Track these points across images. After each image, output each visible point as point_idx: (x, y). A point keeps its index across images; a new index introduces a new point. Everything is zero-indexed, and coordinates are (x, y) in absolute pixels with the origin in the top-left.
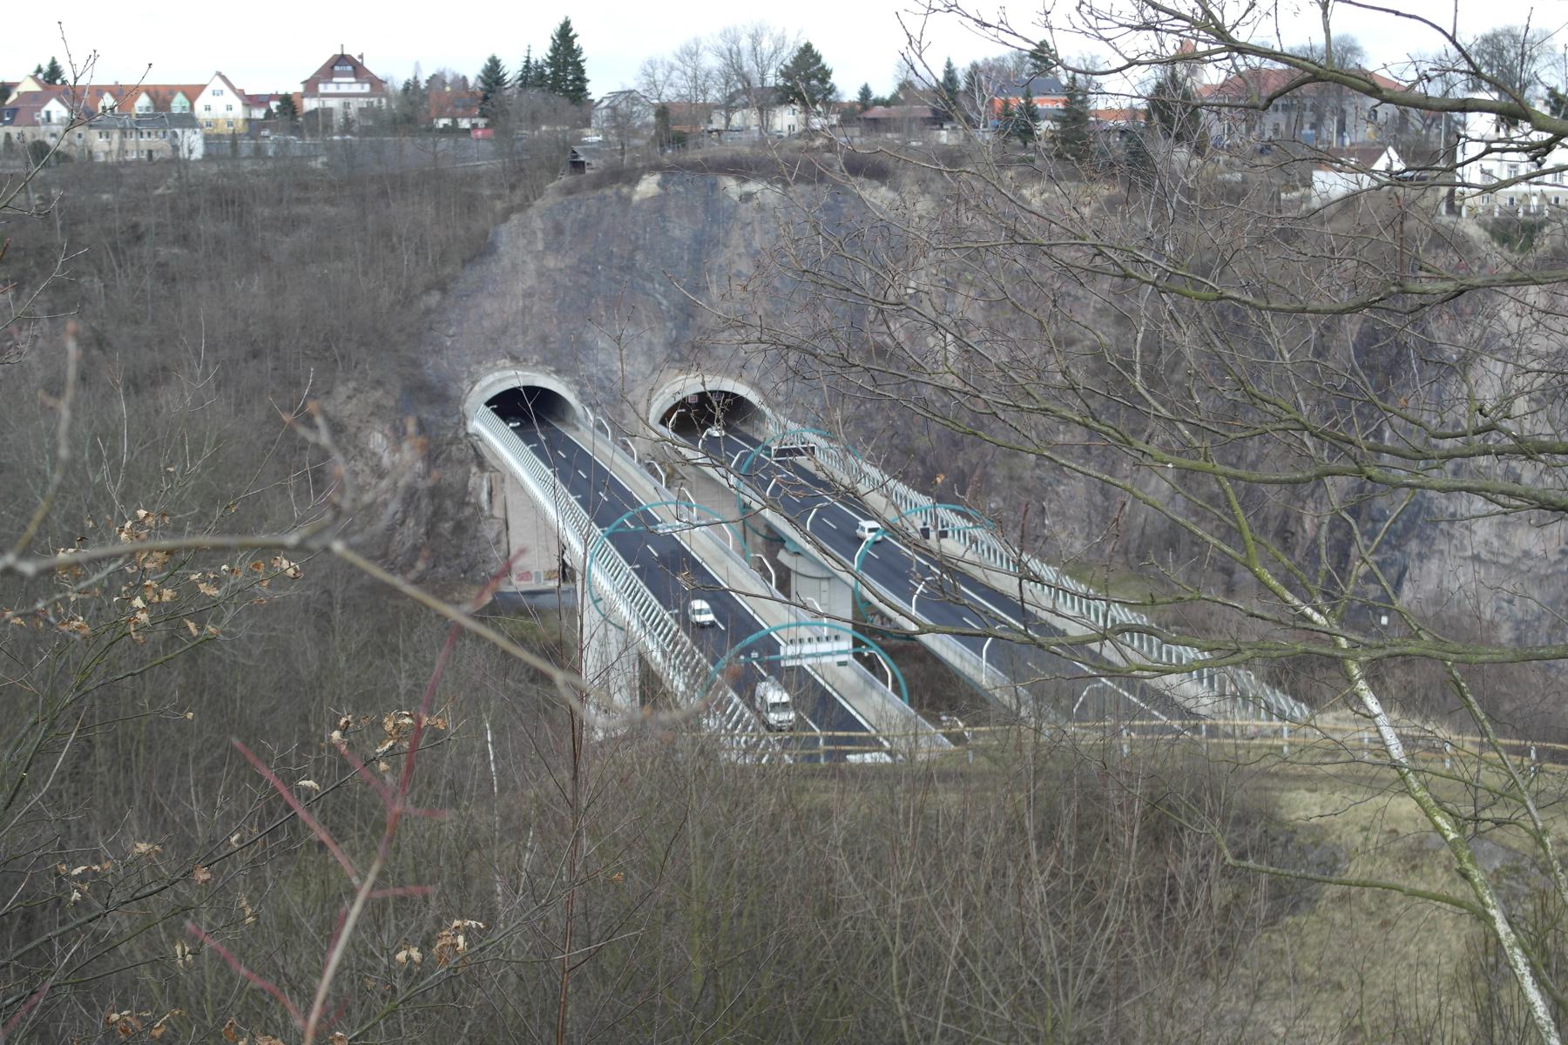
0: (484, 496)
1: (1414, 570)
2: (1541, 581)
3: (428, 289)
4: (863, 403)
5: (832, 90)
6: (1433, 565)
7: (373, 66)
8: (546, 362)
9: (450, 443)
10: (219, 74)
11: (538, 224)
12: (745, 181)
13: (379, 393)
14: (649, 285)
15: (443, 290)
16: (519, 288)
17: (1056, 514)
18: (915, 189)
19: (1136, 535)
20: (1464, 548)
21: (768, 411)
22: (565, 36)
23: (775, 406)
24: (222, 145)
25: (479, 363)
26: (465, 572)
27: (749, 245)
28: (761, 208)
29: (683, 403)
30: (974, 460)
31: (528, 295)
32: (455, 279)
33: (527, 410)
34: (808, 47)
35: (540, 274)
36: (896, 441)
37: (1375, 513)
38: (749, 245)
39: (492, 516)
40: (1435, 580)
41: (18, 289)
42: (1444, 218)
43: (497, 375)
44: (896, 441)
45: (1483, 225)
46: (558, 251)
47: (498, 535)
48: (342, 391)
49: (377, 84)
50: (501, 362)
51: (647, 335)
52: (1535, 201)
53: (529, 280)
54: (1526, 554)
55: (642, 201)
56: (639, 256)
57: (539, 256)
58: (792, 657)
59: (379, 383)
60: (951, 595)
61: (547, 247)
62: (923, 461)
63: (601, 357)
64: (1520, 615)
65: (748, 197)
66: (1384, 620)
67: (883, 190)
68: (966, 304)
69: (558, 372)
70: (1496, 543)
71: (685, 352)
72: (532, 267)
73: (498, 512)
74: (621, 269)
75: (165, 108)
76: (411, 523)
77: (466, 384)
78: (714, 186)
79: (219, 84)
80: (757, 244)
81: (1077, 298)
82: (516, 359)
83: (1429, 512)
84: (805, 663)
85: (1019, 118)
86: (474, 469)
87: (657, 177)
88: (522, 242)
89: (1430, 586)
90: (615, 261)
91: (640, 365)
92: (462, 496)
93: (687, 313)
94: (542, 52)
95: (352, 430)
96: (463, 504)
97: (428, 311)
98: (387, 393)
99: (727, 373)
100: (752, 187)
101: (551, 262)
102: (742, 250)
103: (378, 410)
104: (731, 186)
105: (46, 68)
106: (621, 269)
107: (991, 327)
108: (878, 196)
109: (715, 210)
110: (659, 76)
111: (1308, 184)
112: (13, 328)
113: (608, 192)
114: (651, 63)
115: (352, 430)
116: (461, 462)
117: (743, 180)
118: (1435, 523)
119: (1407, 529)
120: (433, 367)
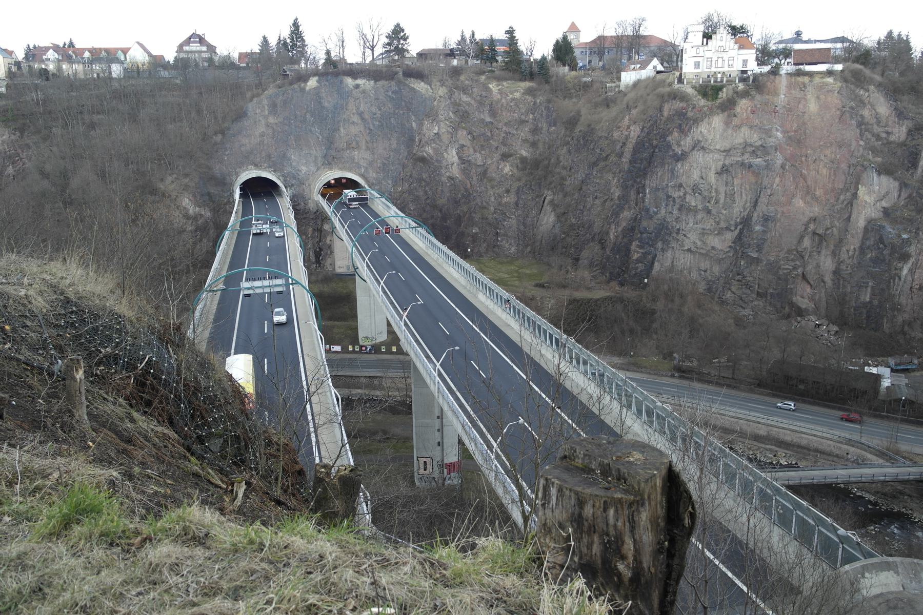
1: (659, 257)
2: (720, 261)
3: (216, 134)
4: (412, 183)
6: (669, 254)
7: (209, 39)
8: (269, 167)
9: (225, 204)
10: (138, 43)
11: (265, 102)
13: (187, 180)
15: (223, 133)
16: (257, 133)
17: (504, 235)
18: (438, 84)
19: (538, 244)
20: (683, 246)
21: (366, 186)
22: (296, 25)
24: (133, 72)
27: (358, 109)
28: (364, 92)
30: (466, 210)
31: (262, 135)
32: (228, 129)
34: (398, 25)
35: (268, 125)
36: (428, 201)
38: (358, 109)
40: (670, 261)
41: (22, 133)
42: (676, 86)
44: (428, 201)
45: (694, 87)
46: (275, 114)
48: (169, 179)
49: (212, 49)
52: (719, 76)
53: (261, 129)
54: (713, 248)
56: (308, 116)
57: (266, 117)
59: (187, 175)
62: (441, 211)
64: (710, 278)
65: (357, 86)
66: (646, 281)
67: (422, 84)
68: (463, 137)
69: (275, 171)
70: (699, 243)
72: (263, 122)
75: (110, 56)
76: (205, 240)
77: (234, 177)
78: (341, 82)
80: (361, 109)
81: (514, 135)
82: (257, 166)
83: (667, 228)
85: (498, 58)
87: (316, 78)
88: (258, 111)
89: (668, 264)
93: (330, 142)
94: (286, 33)
95: (174, 197)
97: (216, 144)
98: (192, 180)
99: (350, 170)
100: (360, 81)
101: (271, 120)
103: (186, 188)
104: (349, 81)
105: (67, 43)
108: (420, 86)
109: (343, 94)
111: (619, 79)
112: (20, 151)
113: (296, 86)
115: (174, 197)
117: (355, 78)
118: (670, 234)
119: (657, 237)
120: (218, 169)
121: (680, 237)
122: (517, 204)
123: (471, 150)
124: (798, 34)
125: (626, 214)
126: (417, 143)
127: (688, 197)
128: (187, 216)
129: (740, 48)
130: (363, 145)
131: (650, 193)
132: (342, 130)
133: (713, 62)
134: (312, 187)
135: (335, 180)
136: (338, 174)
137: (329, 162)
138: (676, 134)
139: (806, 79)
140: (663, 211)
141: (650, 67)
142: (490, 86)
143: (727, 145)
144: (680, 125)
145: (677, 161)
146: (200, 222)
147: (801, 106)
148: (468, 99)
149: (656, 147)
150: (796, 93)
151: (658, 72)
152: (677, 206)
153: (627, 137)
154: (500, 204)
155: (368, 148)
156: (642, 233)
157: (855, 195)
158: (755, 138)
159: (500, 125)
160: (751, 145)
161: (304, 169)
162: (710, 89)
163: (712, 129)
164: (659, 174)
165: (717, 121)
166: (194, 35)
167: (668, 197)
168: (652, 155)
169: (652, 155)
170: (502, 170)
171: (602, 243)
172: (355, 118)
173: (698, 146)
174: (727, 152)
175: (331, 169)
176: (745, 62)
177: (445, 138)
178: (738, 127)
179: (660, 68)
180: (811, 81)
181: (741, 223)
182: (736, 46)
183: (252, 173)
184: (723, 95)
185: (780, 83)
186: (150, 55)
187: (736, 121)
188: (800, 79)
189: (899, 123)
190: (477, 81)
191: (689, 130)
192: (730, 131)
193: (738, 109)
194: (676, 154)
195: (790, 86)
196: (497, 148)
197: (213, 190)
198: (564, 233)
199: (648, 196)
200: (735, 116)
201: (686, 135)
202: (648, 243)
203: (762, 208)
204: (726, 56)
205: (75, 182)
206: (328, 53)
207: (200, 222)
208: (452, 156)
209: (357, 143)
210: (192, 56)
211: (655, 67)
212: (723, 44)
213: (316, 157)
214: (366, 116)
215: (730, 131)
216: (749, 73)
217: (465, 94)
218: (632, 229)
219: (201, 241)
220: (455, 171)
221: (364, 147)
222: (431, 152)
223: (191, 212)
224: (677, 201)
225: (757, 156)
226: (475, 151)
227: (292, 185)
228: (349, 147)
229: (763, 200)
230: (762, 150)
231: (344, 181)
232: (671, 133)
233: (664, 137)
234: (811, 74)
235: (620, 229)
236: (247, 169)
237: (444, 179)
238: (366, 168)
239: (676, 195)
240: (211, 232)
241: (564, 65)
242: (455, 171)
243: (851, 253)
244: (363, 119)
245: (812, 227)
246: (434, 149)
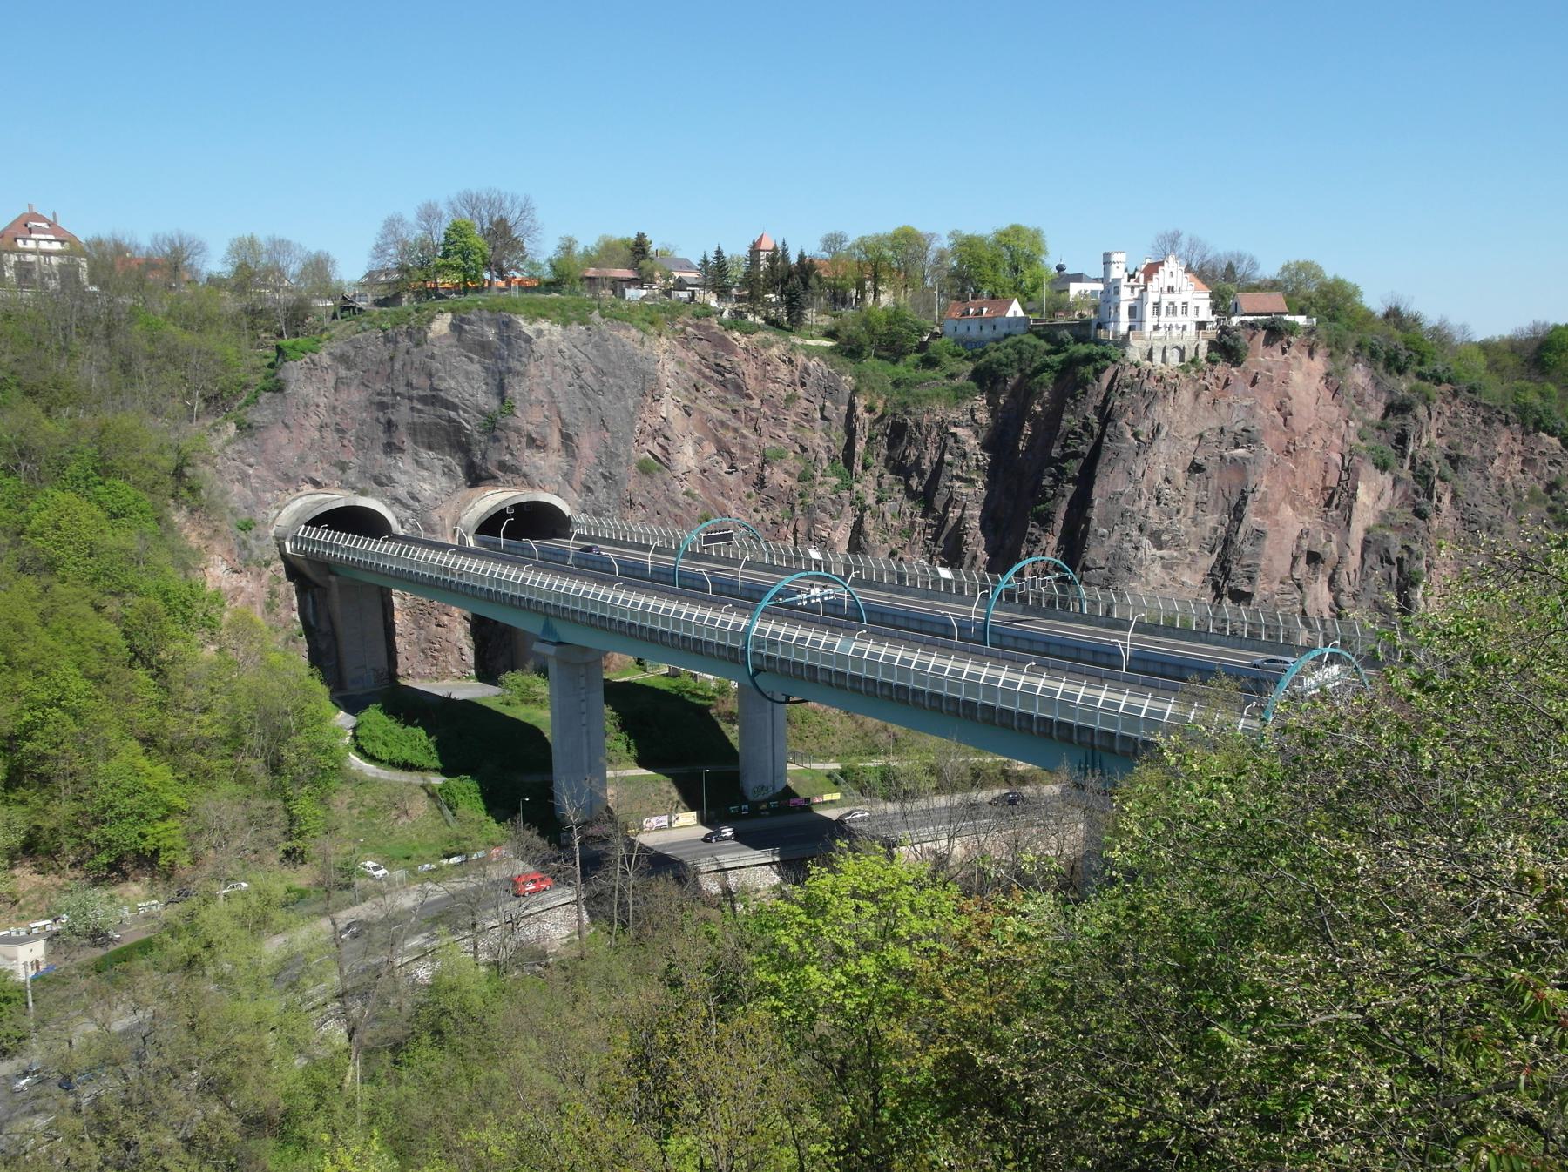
12: (534, 320)
65: (540, 333)
100: (544, 325)
124: (1060, 268)
130: (555, 440)
157: (1353, 496)
183: (337, 498)
203: (1251, 519)
209: (544, 439)
210: (31, 258)
212: (1171, 282)
229: (1250, 508)
230: (1245, 437)
243: (1352, 576)
245: (1305, 543)
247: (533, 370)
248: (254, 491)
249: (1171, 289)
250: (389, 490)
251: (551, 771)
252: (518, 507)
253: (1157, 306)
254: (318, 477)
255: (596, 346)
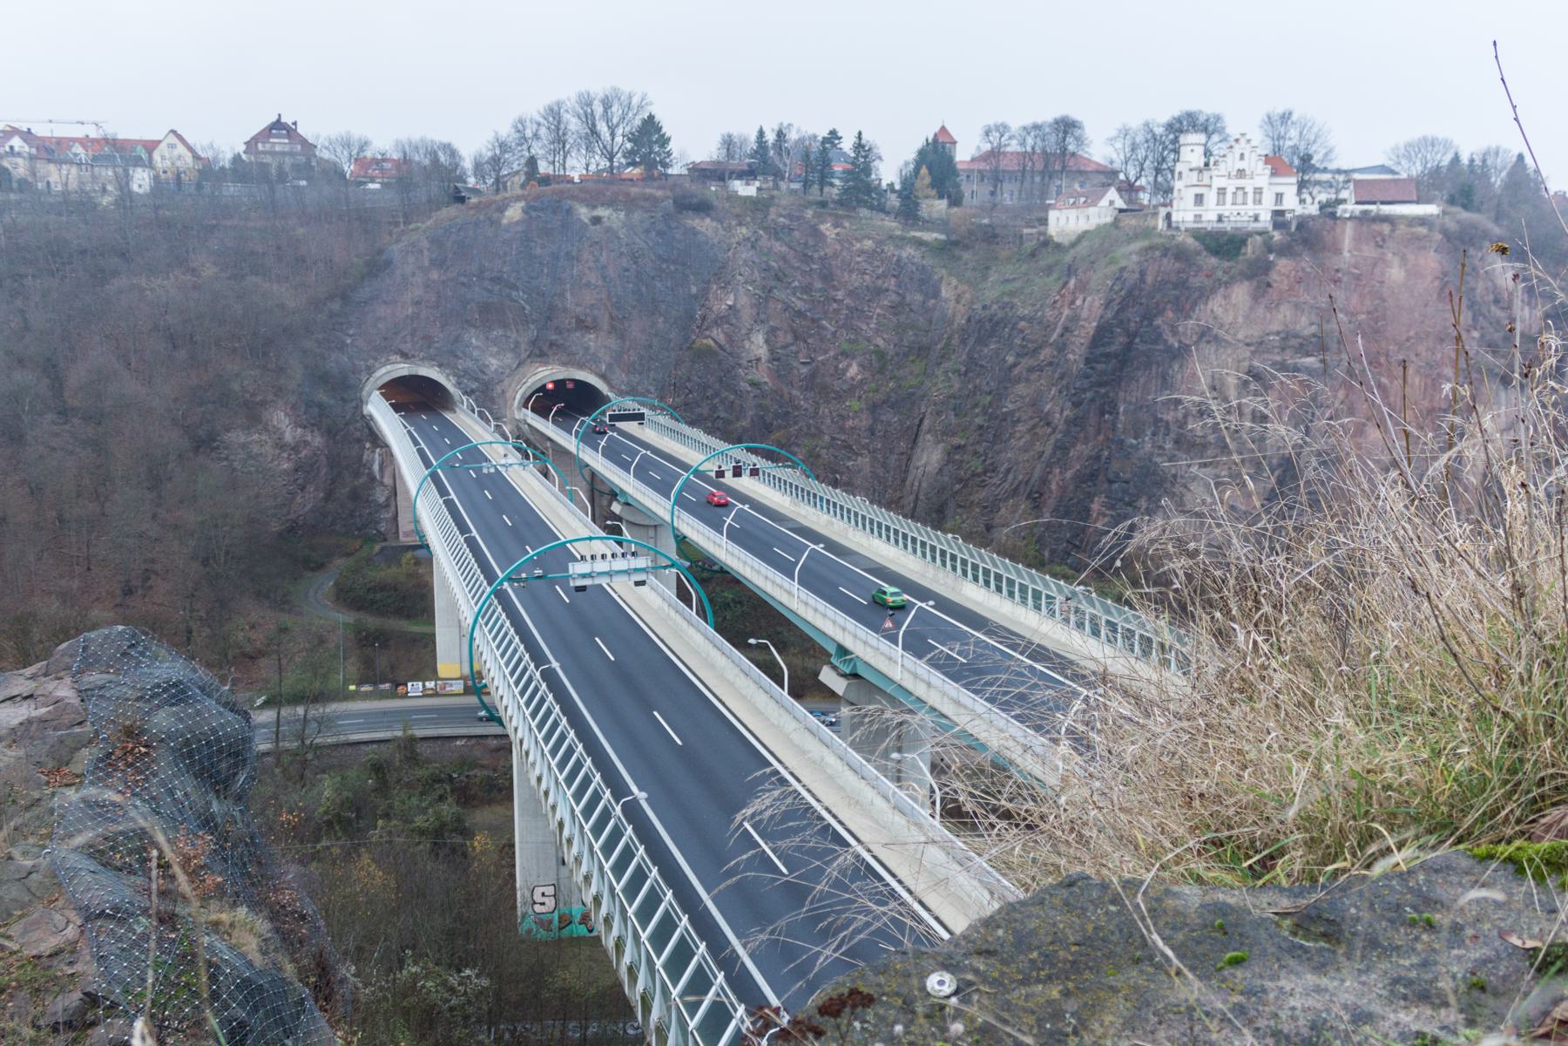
0: (376, 467)
5: (669, 154)
10: (173, 132)
12: (594, 207)
14: (514, 294)
15: (344, 297)
16: (408, 297)
21: (611, 395)
23: (621, 393)
25: (376, 359)
26: (359, 529)
28: (609, 230)
29: (543, 388)
33: (416, 398)
37: (1111, 476)
39: (382, 483)
43: (389, 367)
47: (388, 499)
50: (393, 358)
51: (514, 336)
53: (418, 292)
55: (510, 224)
58: (584, 576)
60: (760, 535)
61: (433, 262)
63: (476, 353)
65: (597, 220)
67: (708, 220)
69: (440, 366)
71: (545, 348)
73: (387, 480)
74: (491, 280)
79: (172, 139)
82: (405, 356)
84: (603, 581)
86: (368, 445)
87: (522, 204)
90: (487, 274)
91: (509, 359)
92: (360, 467)
96: (357, 475)
99: (581, 366)
100: (602, 212)
101: (435, 275)
102: (591, 264)
104: (583, 213)
106: (491, 280)
107: (794, 332)
110: (529, 133)
114: (521, 121)
116: (359, 441)
120: (335, 361)
121: (1177, 489)
122: (872, 431)
123: (789, 338)
125: (1082, 449)
126: (699, 322)
127: (1190, 419)
128: (281, 446)
129: (1274, 174)
130: (605, 323)
131: (1125, 411)
132: (568, 295)
133: (1229, 197)
134: (508, 395)
135: (556, 383)
136: (561, 373)
137: (540, 352)
138: (1170, 314)
139: (1386, 228)
140: (1148, 447)
141: (1104, 202)
142: (822, 227)
143: (1254, 332)
144: (1177, 298)
145: (1174, 358)
146: (303, 455)
147: (1377, 270)
148: (784, 249)
149: (1135, 335)
150: (1369, 251)
151: (1121, 211)
152: (1172, 435)
153: (1075, 318)
154: (842, 430)
155: (613, 330)
156: (1111, 482)
158: (1305, 325)
159: (840, 295)
160: (1296, 336)
161: (494, 363)
162: (1224, 244)
163: (1231, 307)
164: (1142, 380)
165: (1241, 293)
166: (278, 125)
167: (1157, 421)
168: (1129, 347)
169: (1129, 347)
170: (845, 370)
171: (1036, 500)
172: (593, 278)
173: (1205, 335)
174: (1259, 346)
175: (546, 364)
176: (1279, 197)
177: (747, 315)
178: (1273, 307)
179: (1120, 204)
180: (1393, 231)
181: (1280, 465)
182: (1268, 172)
183: (402, 369)
184: (1249, 250)
185: (1344, 232)
186: (196, 157)
187: (1273, 293)
188: (1376, 227)
189: (1529, 304)
190: (798, 218)
191: (1192, 308)
192: (1261, 311)
193: (1274, 276)
194: (1169, 349)
195: (1358, 240)
196: (834, 334)
197: (322, 396)
198: (960, 480)
199: (1122, 418)
200: (1269, 285)
201: (1188, 317)
202: (1121, 500)
204: (1249, 185)
205: (76, 376)
206: (532, 162)
207: (303, 455)
208: (758, 345)
209: (595, 320)
211: (1111, 203)
212: (1241, 165)
213: (517, 343)
214: (611, 272)
215: (1261, 311)
216: (1288, 216)
217: (778, 239)
218: (1093, 476)
219: (303, 489)
220: (762, 375)
221: (606, 327)
222: (721, 338)
223: (288, 437)
224: (1173, 427)
225: (1308, 355)
226: (796, 338)
227: (473, 391)
228: (583, 325)
231: (570, 386)
232: (1161, 312)
233: (1148, 317)
234: (1387, 219)
235: (1069, 475)
236: (388, 362)
237: (744, 386)
238: (610, 366)
239: (1169, 417)
240: (323, 472)
241: (941, 197)
242: (762, 375)
244: (604, 278)
246: (728, 336)
247: (586, 255)
248: (350, 358)
249: (1241, 173)
250: (461, 364)
251: (433, 624)
252: (559, 384)
253: (1222, 191)
254: (407, 347)
255: (659, 233)
